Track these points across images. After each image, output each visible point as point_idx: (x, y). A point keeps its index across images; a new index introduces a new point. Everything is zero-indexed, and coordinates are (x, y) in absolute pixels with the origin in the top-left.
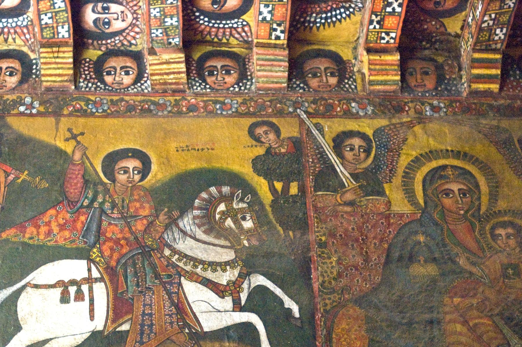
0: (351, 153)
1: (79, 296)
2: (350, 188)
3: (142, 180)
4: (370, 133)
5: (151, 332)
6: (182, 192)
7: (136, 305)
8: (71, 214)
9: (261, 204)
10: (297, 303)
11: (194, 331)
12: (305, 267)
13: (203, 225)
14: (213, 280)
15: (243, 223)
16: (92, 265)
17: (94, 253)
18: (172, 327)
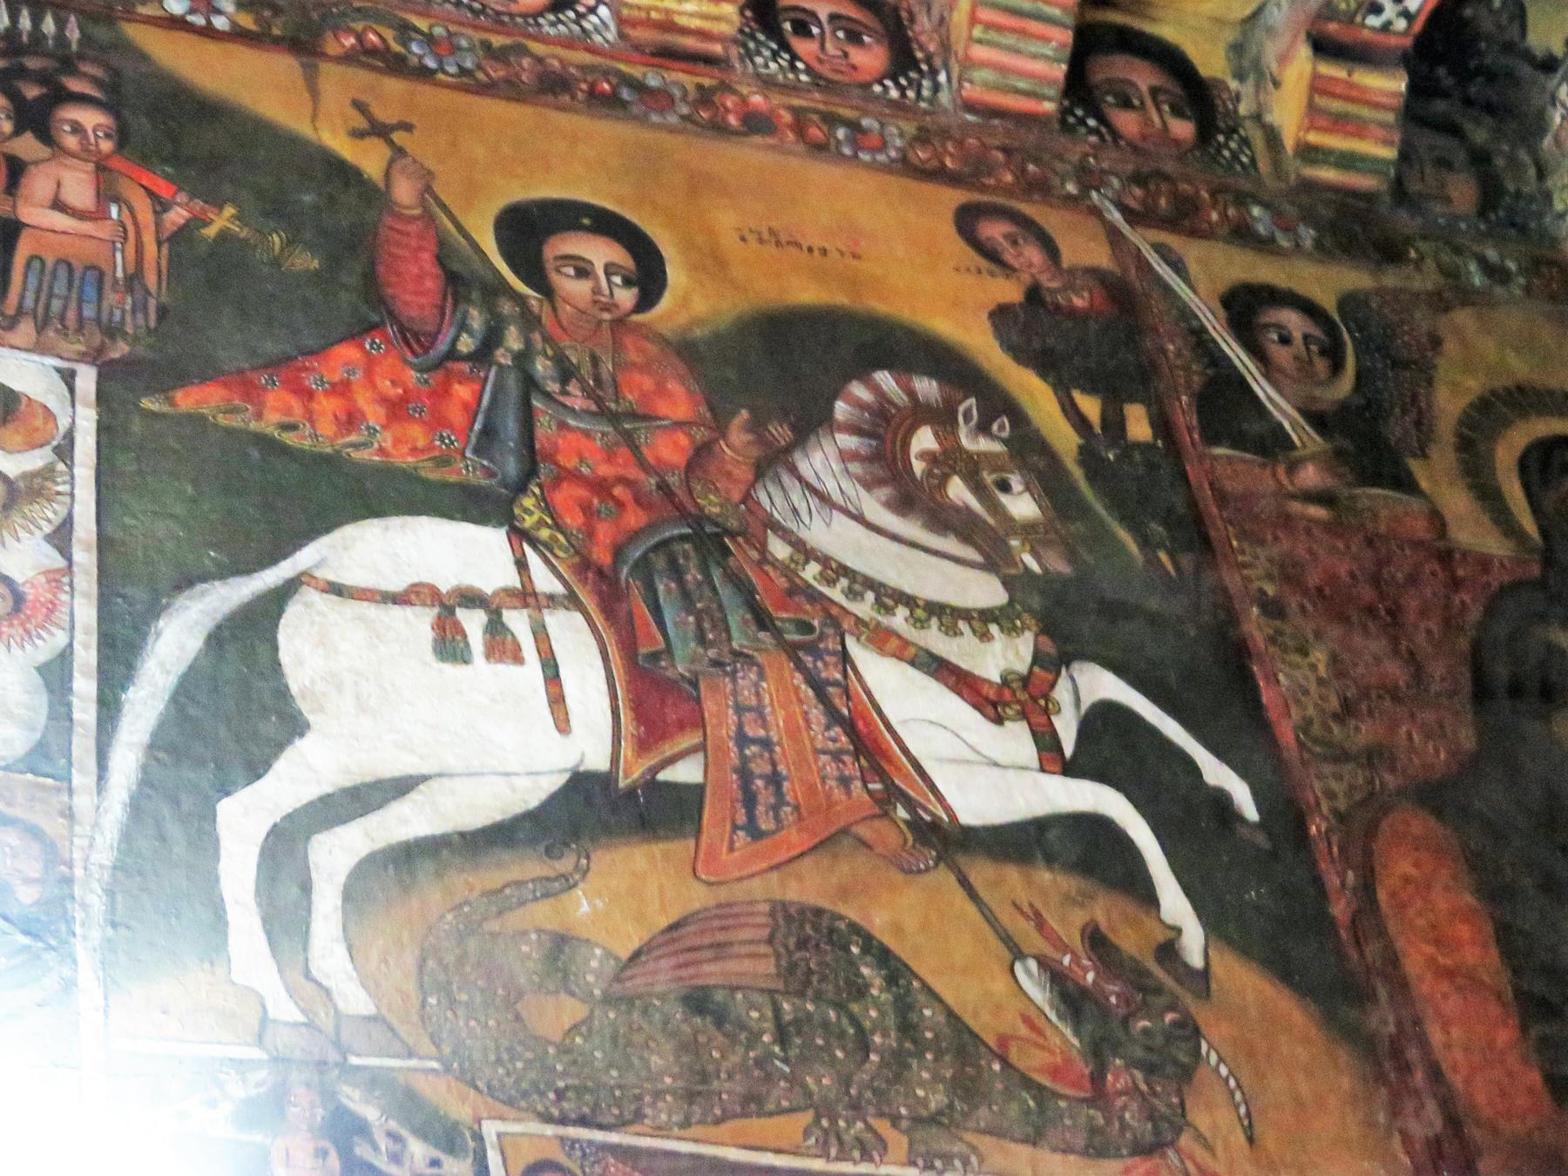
1: (501, 647)
2: (1307, 452)
4: (1329, 302)
7: (709, 706)
8: (421, 371)
11: (928, 818)
15: (1004, 499)
16: (526, 547)
17: (526, 511)
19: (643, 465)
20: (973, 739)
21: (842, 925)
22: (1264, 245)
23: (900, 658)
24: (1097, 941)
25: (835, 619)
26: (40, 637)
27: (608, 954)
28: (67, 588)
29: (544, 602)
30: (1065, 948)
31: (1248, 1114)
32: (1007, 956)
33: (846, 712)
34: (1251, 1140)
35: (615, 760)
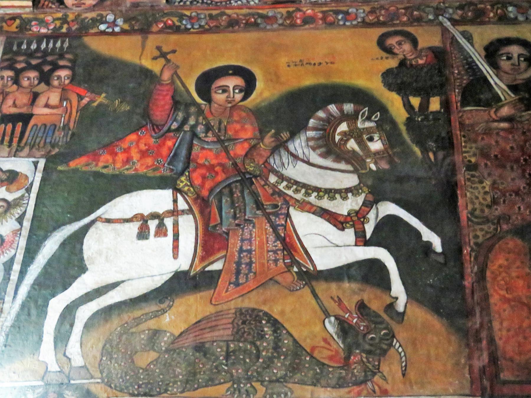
0: (509, 63)
1: (161, 231)
2: (507, 101)
3: (244, 98)
5: (250, 270)
6: (292, 112)
7: (231, 241)
8: (156, 139)
9: (393, 123)
10: (438, 235)
11: (305, 270)
12: (450, 193)
13: (319, 147)
14: (330, 209)
16: (179, 195)
17: (182, 182)
18: (276, 265)
19: (229, 158)
20: (330, 238)
21: (261, 314)
22: (514, 22)
23: (309, 212)
24: (362, 307)
25: (288, 202)
26: (6, 253)
27: (172, 334)
28: (19, 235)
29: (180, 212)
30: (347, 310)
31: (406, 366)
32: (324, 317)
33: (283, 235)
34: (404, 375)
35: (191, 266)
